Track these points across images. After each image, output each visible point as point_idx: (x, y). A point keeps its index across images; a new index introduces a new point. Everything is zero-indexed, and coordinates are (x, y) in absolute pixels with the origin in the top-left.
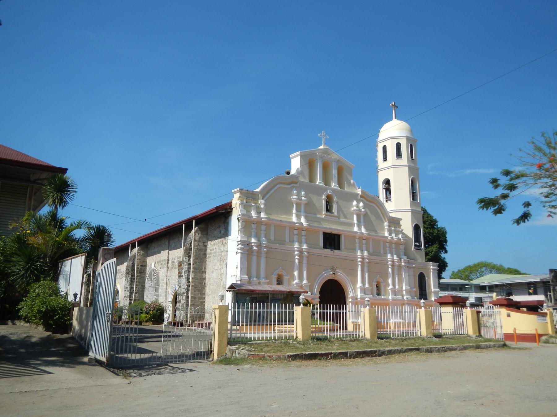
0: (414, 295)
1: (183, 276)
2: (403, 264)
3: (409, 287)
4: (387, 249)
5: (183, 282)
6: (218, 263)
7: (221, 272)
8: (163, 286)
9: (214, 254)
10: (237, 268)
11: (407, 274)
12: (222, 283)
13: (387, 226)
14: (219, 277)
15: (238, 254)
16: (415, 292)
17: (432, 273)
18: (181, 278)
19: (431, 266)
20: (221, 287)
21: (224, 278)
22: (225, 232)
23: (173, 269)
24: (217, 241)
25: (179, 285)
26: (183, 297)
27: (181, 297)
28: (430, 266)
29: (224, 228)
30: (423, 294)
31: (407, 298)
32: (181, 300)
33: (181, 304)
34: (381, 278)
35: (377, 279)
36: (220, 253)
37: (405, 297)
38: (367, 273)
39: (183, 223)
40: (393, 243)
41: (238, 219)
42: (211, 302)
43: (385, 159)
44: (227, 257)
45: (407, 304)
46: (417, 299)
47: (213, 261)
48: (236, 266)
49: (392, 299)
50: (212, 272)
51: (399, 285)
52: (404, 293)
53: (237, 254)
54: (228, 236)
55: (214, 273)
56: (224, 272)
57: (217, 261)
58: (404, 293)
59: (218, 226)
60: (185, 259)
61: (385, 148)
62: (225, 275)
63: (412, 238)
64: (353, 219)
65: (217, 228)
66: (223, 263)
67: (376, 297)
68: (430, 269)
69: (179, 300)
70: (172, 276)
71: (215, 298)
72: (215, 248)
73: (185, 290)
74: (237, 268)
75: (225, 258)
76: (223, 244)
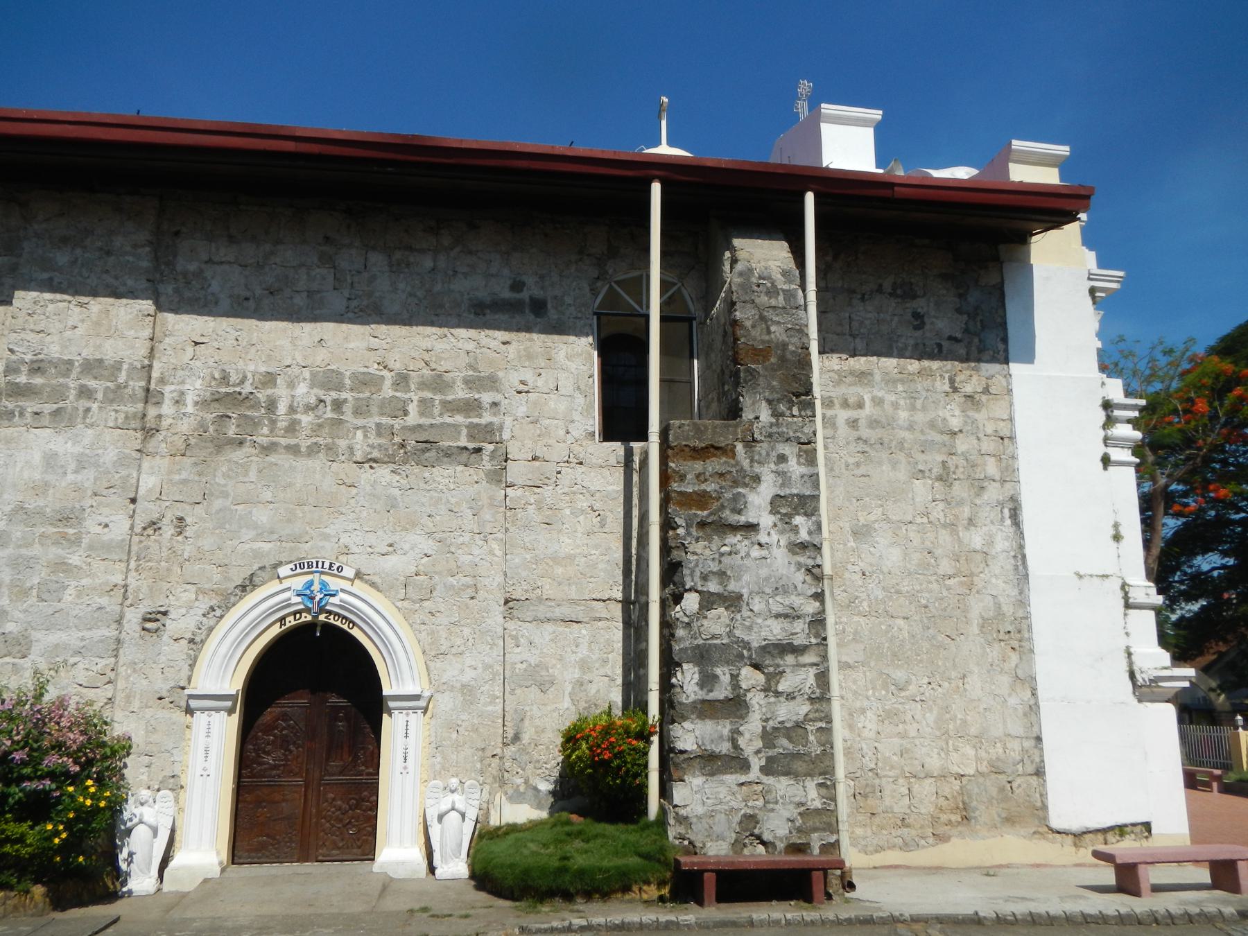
1: (752, 528)
5: (764, 572)
6: (922, 490)
7: (960, 540)
8: (62, 566)
9: (865, 432)
10: (1117, 538)
12: (978, 607)
14: (946, 566)
15: (1110, 468)
18: (734, 539)
20: (975, 629)
21: (1000, 582)
22: (966, 331)
23: (247, 449)
24: (890, 363)
25: (713, 587)
26: (773, 677)
27: (750, 677)
29: (959, 311)
32: (756, 700)
33: (752, 726)
36: (939, 438)
39: (657, 173)
41: (1092, 291)
42: (863, 711)
44: (1009, 474)
47: (862, 470)
48: (1112, 532)
50: (862, 533)
53: (1105, 468)
54: (1006, 361)
55: (883, 539)
56: (990, 542)
57: (902, 474)
59: (887, 285)
60: (776, 414)
62: (1002, 563)
65: (880, 290)
66: (978, 495)
69: (721, 692)
70: (218, 503)
71: (912, 689)
72: (878, 402)
73: (799, 626)
74: (1117, 538)
75: (992, 468)
76: (955, 390)
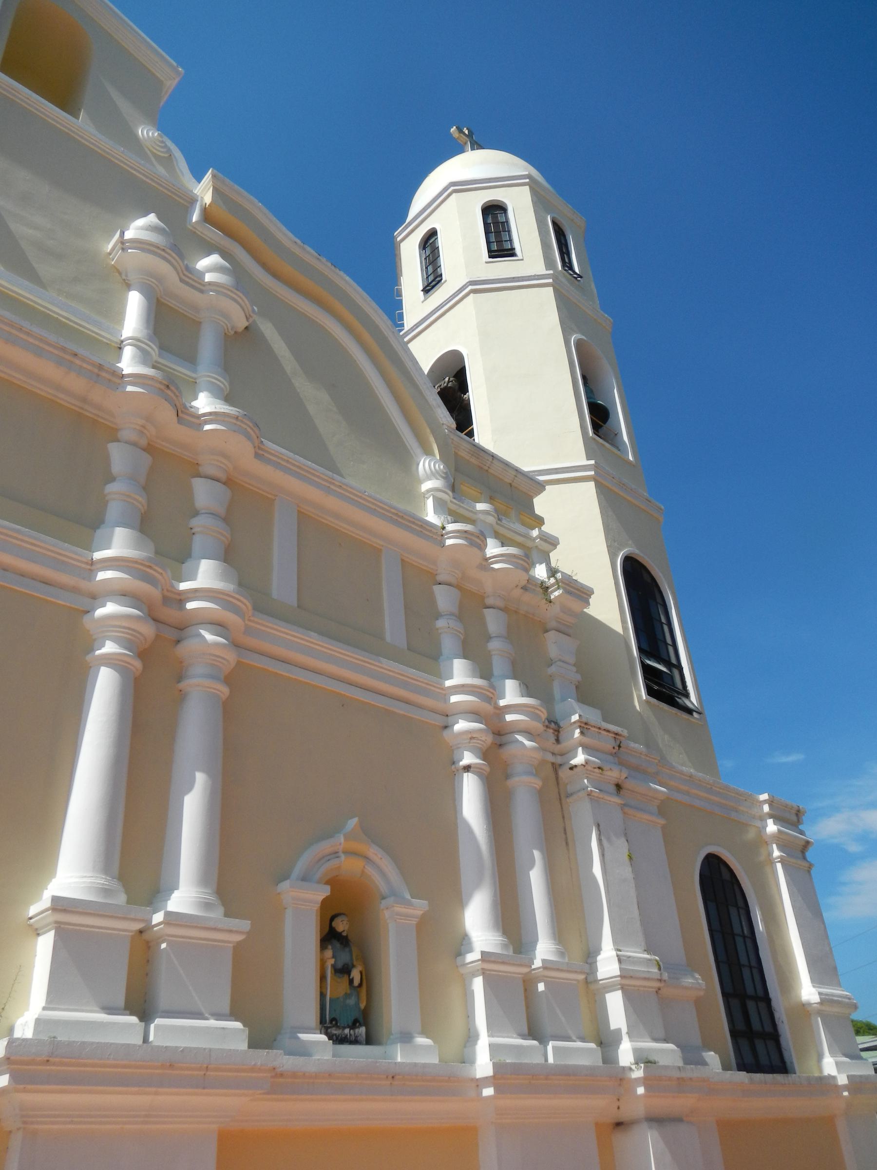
0: (696, 1039)
2: (580, 758)
3: (647, 951)
4: (441, 623)
11: (621, 847)
13: (433, 475)
16: (698, 1003)
17: (779, 866)
19: (770, 822)
28: (763, 818)
30: (756, 1026)
31: (643, 1059)
34: (374, 852)
35: (335, 854)
37: (626, 1054)
38: (200, 778)
40: (490, 601)
43: (432, 282)
45: (656, 1120)
46: (726, 1067)
49: (498, 1067)
51: (559, 934)
52: (615, 1003)
58: (615, 1003)
61: (429, 241)
63: (619, 628)
64: (119, 317)
67: (304, 1051)
68: (762, 841)
